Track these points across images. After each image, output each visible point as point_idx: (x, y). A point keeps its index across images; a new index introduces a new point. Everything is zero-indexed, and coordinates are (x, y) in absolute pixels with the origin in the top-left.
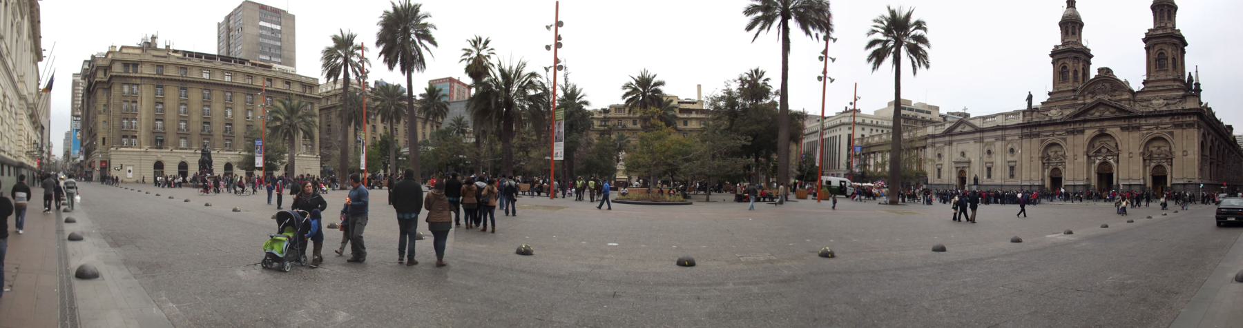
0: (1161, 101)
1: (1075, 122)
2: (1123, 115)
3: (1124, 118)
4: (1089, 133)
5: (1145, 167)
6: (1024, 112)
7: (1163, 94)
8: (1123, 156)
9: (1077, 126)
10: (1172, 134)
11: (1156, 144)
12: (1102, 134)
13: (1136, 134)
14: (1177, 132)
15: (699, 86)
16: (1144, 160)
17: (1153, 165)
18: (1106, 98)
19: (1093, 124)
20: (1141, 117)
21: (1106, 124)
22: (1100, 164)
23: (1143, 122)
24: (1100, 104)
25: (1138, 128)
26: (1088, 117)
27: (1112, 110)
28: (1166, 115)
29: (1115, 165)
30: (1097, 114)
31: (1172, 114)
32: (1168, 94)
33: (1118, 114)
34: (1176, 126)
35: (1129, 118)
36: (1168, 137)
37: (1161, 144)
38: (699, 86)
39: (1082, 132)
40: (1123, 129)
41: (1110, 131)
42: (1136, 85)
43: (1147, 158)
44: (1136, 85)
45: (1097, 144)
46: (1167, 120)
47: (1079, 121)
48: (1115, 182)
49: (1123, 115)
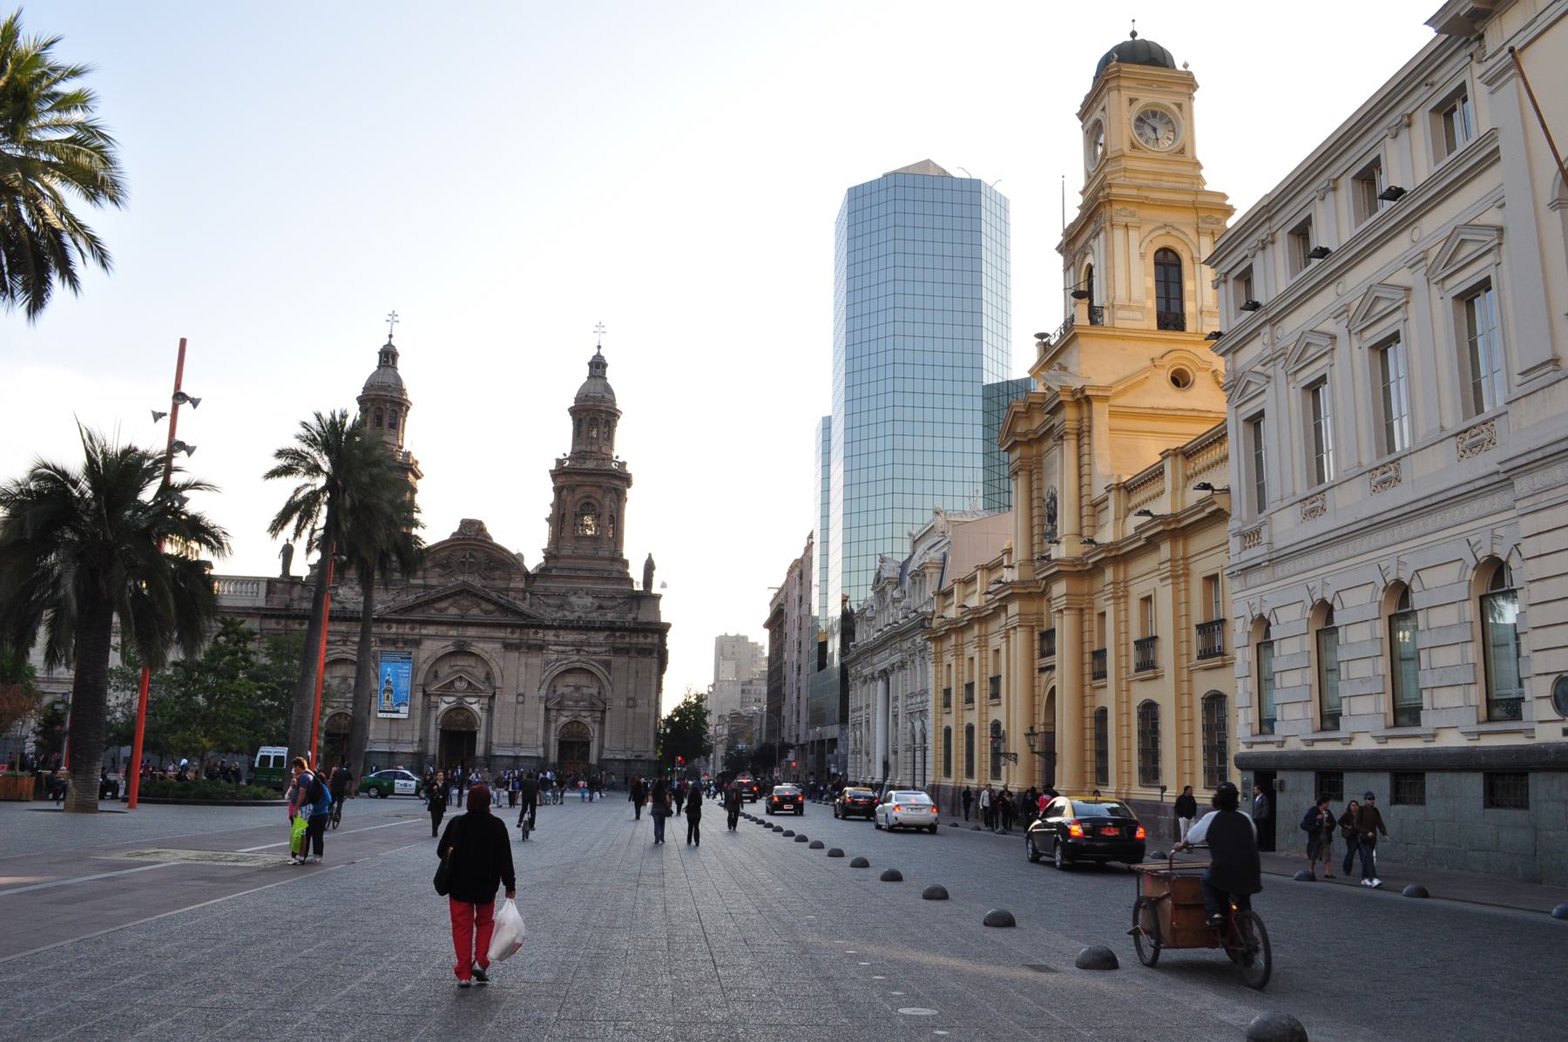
0: (588, 601)
1: (399, 622)
2: (511, 619)
3: (514, 626)
4: (431, 649)
5: (547, 721)
6: (271, 582)
7: (588, 585)
8: (506, 698)
9: (406, 629)
10: (607, 664)
11: (571, 680)
12: (461, 651)
13: (536, 660)
14: (619, 661)
15: (183, 342)
16: (547, 710)
17: (563, 720)
18: (476, 582)
19: (443, 629)
20: (548, 627)
21: (471, 632)
22: (449, 711)
23: (550, 636)
24: (465, 592)
25: (541, 648)
26: (432, 613)
27: (484, 605)
28: (600, 629)
29: (483, 716)
30: (453, 611)
31: (611, 628)
32: (599, 587)
33: (498, 617)
34: (617, 651)
35: (521, 627)
36: (599, 671)
37: (582, 680)
38: (183, 342)
39: (417, 643)
40: (508, 646)
41: (477, 648)
42: (533, 560)
43: (553, 705)
44: (533, 560)
45: (445, 670)
46: (601, 637)
47: (413, 621)
48: (480, 750)
49: (511, 619)
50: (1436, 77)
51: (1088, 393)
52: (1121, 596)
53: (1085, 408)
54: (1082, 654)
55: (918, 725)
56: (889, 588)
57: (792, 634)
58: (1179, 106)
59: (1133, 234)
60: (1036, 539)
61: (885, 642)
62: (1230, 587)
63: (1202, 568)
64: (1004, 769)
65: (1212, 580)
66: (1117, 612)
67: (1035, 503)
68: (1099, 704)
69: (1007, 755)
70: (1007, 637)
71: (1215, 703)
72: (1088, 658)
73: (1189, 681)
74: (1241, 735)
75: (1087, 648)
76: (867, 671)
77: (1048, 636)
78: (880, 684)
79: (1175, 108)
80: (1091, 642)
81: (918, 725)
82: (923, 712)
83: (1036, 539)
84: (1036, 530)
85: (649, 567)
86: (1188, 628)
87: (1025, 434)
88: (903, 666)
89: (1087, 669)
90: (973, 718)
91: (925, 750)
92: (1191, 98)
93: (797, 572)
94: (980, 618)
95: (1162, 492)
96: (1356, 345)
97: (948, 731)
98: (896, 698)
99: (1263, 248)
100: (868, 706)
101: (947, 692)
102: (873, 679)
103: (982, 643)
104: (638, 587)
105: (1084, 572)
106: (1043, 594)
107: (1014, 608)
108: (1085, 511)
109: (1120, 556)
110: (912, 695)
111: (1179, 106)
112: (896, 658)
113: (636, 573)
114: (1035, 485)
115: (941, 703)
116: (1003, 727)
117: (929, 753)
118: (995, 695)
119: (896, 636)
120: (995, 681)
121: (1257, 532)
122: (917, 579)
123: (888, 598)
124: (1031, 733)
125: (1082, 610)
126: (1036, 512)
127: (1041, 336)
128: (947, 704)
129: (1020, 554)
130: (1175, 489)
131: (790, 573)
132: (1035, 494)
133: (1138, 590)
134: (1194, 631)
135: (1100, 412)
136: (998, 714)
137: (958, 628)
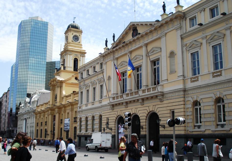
50: (101, 60)
51: (62, 81)
52: (65, 112)
53: (62, 84)
54: (59, 120)
55: (32, 129)
56: (27, 104)
58: (80, 35)
59: (71, 56)
60: (54, 101)
61: (26, 113)
62: (78, 113)
63: (75, 110)
64: (47, 136)
65: (76, 112)
66: (64, 114)
67: (54, 95)
68: (61, 127)
69: (48, 134)
70: (48, 116)
71: (75, 128)
72: (60, 120)
73: (73, 125)
74: (78, 132)
75: (60, 119)
76: (22, 118)
77: (55, 116)
78: (25, 121)
79: (79, 36)
80: (61, 118)
81: (32, 129)
82: (33, 127)
83: (54, 101)
84: (54, 100)
86: (73, 118)
87: (52, 84)
88: (29, 118)
89: (60, 122)
90: (42, 128)
91: (33, 133)
92: (81, 34)
93: (5, 95)
94: (44, 112)
95: (71, 98)
97: (37, 130)
98: (28, 124)
99: (84, 71)
100: (22, 125)
101: (38, 123)
102: (23, 120)
103: (44, 116)
105: (59, 108)
106: (54, 110)
107: (50, 111)
108: (61, 98)
109: (65, 106)
110: (31, 123)
111: (80, 35)
112: (28, 116)
114: (54, 92)
115: (36, 125)
116: (47, 130)
117: (34, 134)
118: (46, 125)
119: (28, 113)
120: (46, 122)
121: (81, 107)
122: (33, 103)
123: (27, 106)
124: (51, 131)
125: (59, 113)
126: (54, 97)
128: (38, 125)
129: (51, 103)
130: (72, 98)
131: (4, 95)
132: (54, 94)
133: (67, 111)
134: (73, 118)
135: (64, 85)
136: (46, 128)
137: (40, 113)
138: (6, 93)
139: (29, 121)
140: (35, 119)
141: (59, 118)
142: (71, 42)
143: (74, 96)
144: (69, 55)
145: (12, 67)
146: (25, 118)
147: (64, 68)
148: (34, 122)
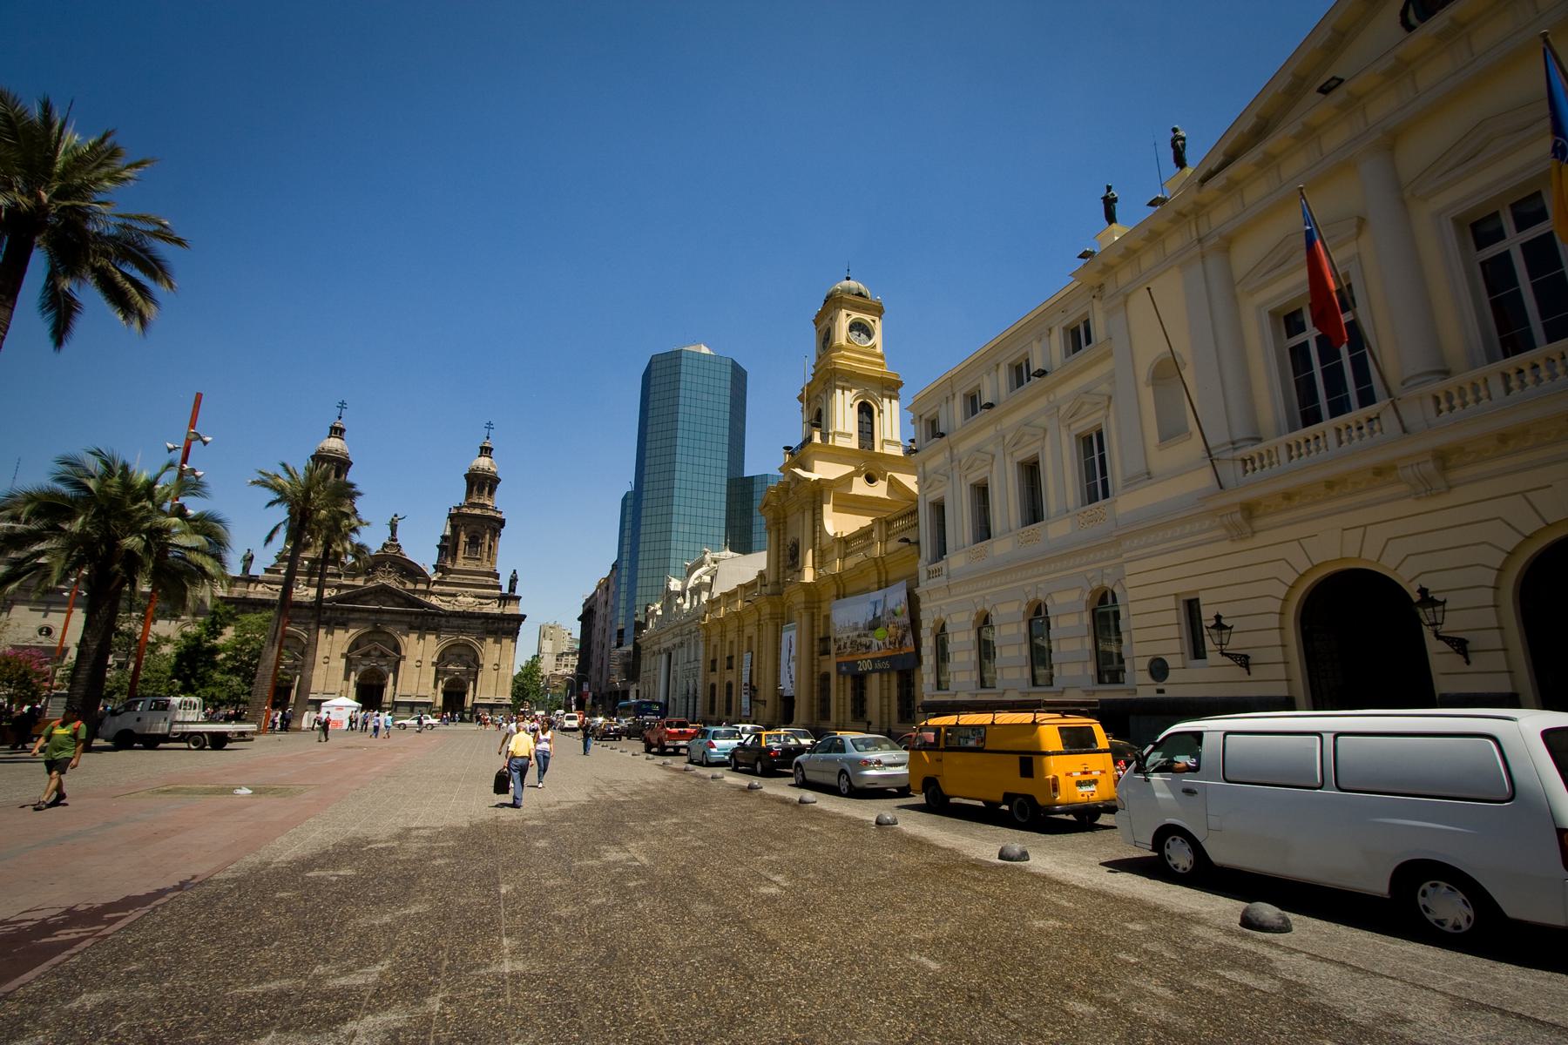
41: (390, 629)
54: (813, 640)
57: (599, 623)
68: (823, 670)
76: (655, 648)
78: (664, 657)
81: (691, 682)
85: (513, 581)
96: (1008, 460)
97: (713, 687)
101: (714, 662)
104: (505, 590)
113: (504, 582)
127: (787, 448)
128: (713, 670)
131: (599, 586)
138: (607, 579)
139: (680, 656)
140: (701, 646)
141: (813, 633)
142: (844, 342)
143: (888, 529)
144: (839, 392)
145: (624, 500)
146: (665, 646)
147: (824, 436)
148: (701, 657)
